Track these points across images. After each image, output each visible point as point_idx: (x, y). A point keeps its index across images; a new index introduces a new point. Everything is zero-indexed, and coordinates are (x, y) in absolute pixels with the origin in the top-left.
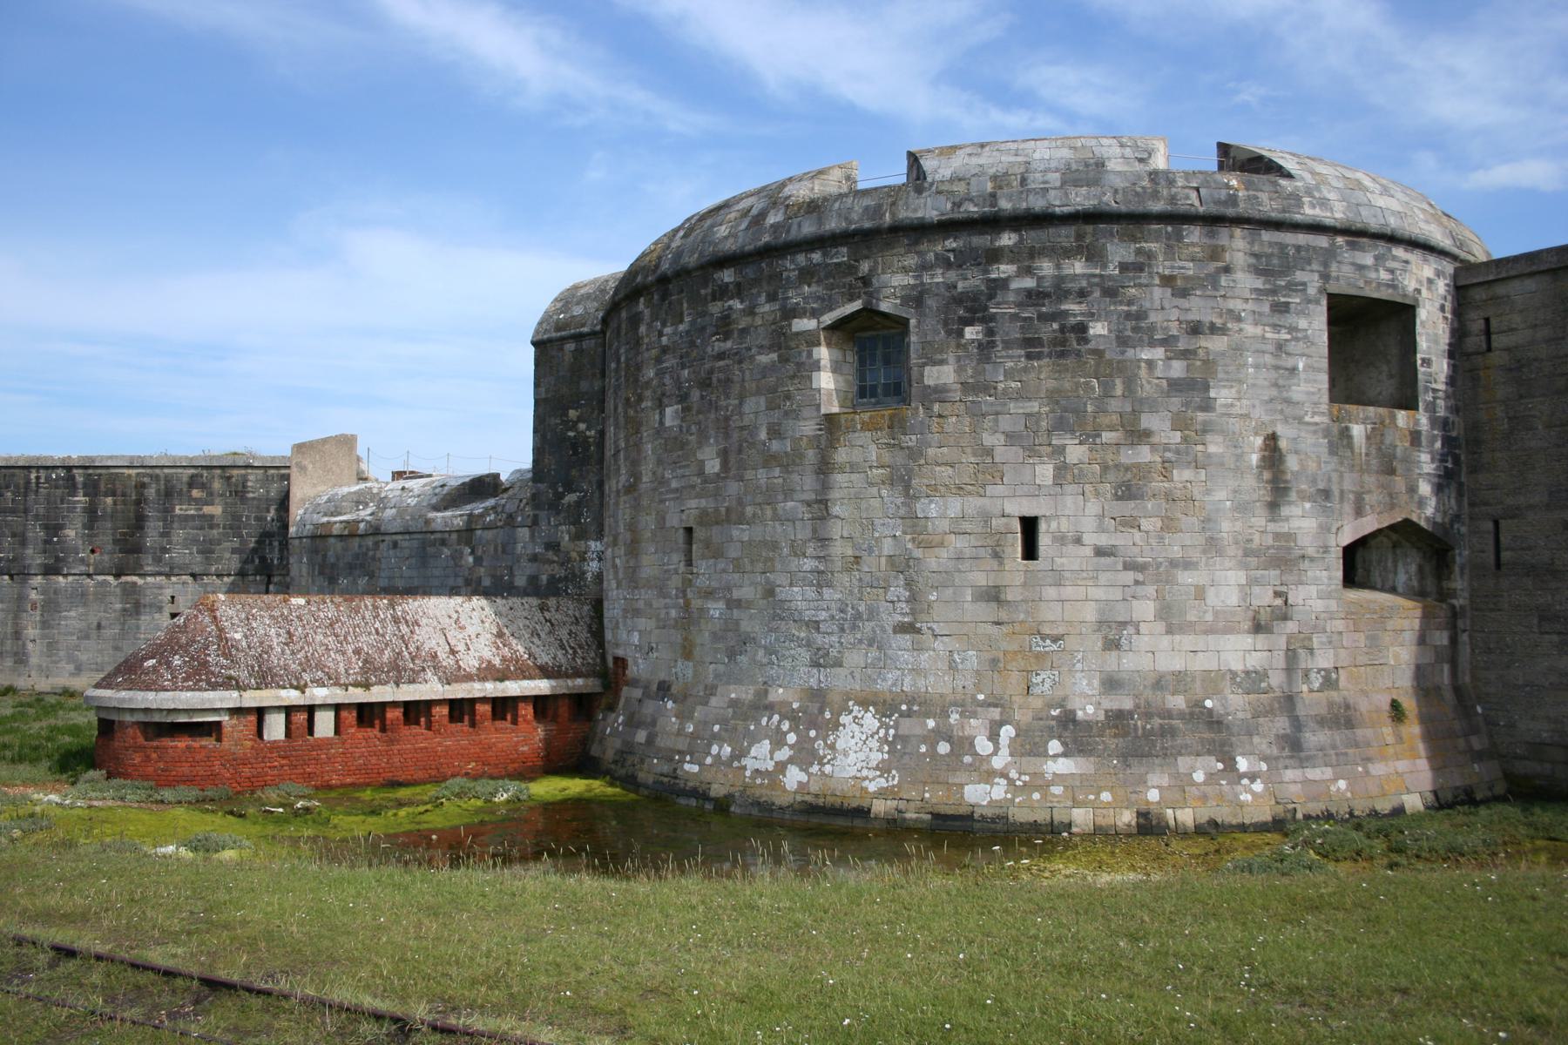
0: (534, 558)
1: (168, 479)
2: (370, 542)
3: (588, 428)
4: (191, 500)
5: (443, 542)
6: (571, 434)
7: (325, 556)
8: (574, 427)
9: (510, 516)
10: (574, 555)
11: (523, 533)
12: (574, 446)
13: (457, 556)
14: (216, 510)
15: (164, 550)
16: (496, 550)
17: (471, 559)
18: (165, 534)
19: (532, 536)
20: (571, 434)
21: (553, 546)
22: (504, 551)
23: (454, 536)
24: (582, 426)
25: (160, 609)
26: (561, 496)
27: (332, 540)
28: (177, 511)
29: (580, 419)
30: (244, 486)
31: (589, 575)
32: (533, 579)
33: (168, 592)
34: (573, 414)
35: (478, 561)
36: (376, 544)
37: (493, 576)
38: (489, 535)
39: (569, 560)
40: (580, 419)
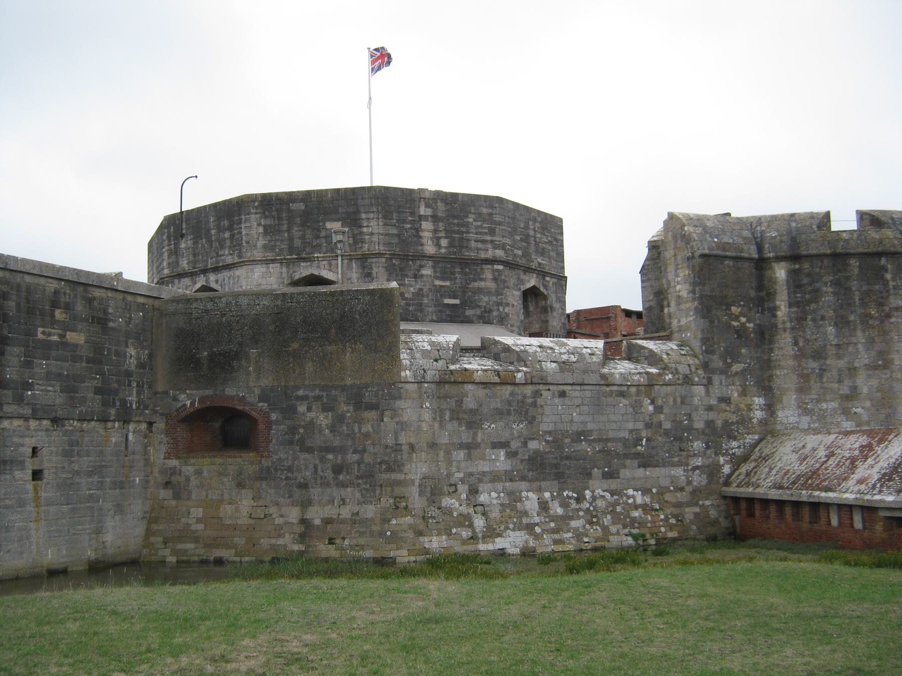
0: (710, 408)
1: (29, 290)
2: (529, 390)
3: (749, 321)
4: (53, 322)
5: (622, 394)
6: (735, 324)
7: (460, 402)
8: (737, 318)
9: (686, 377)
10: (742, 406)
11: (699, 390)
12: (737, 332)
13: (637, 407)
14: (76, 337)
15: (28, 386)
16: (675, 401)
17: (651, 408)
18: (28, 364)
19: (707, 393)
20: (735, 324)
21: (725, 400)
22: (683, 402)
23: (633, 390)
24: (743, 320)
25: (21, 464)
26: (729, 366)
27: (470, 387)
28: (40, 336)
29: (742, 314)
30: (105, 312)
31: (755, 421)
32: (710, 424)
33: (30, 442)
34: (735, 310)
35: (659, 410)
36: (537, 394)
37: (673, 421)
38: (669, 389)
39: (739, 409)
40: (742, 314)
